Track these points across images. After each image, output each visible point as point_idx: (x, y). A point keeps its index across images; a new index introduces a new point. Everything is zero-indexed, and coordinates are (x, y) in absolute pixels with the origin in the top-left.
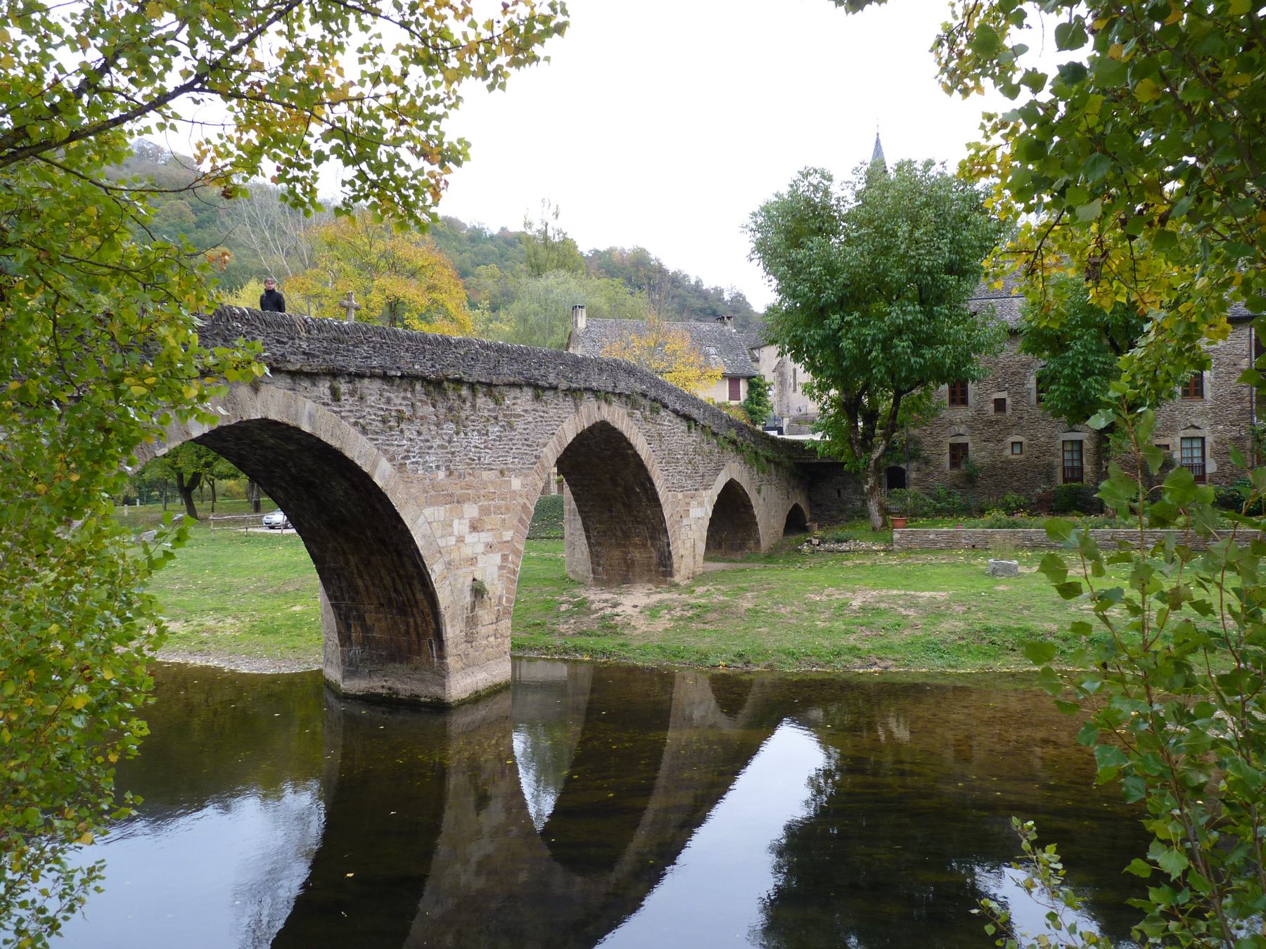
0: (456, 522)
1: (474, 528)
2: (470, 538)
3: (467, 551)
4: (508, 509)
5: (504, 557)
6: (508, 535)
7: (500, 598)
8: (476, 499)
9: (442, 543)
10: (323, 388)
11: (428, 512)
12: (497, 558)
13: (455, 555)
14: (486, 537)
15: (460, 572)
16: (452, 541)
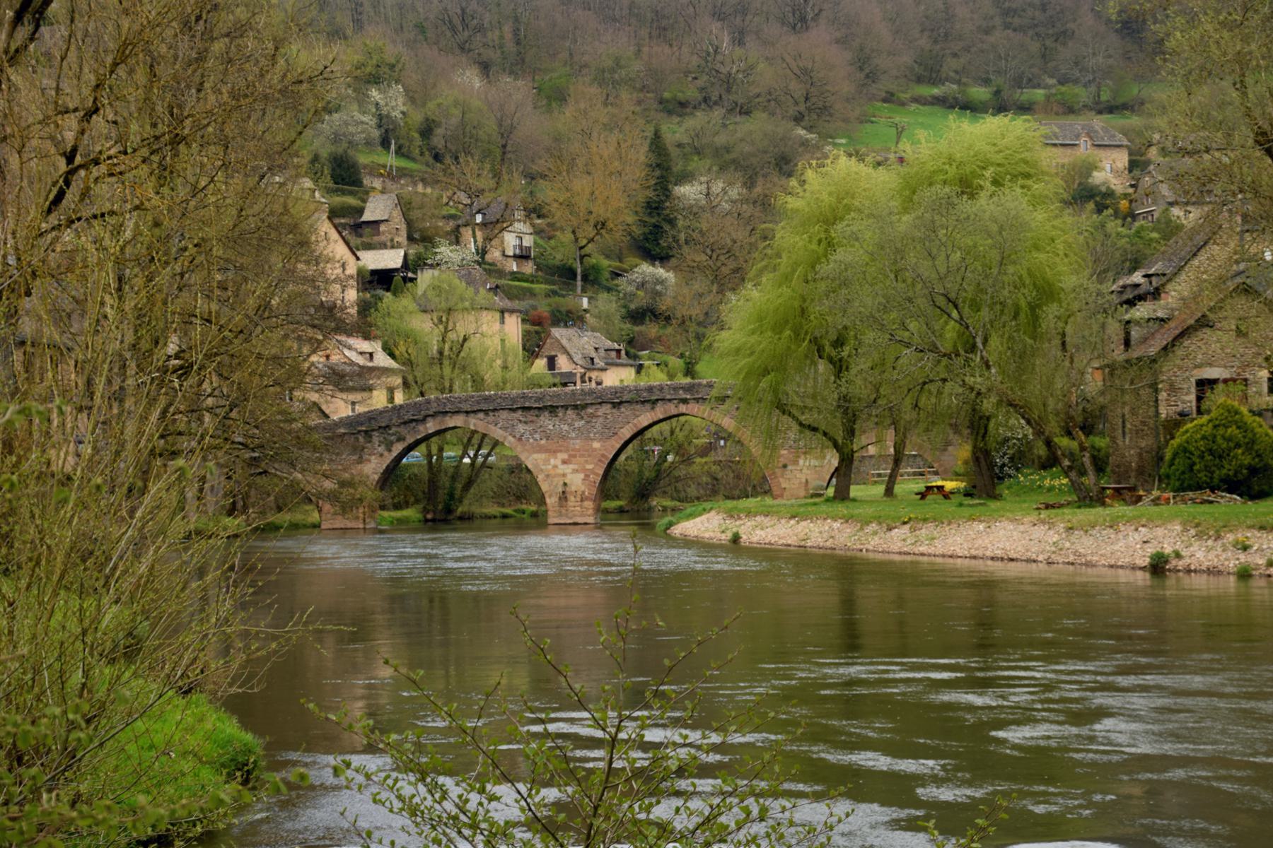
0: (552, 461)
1: (564, 462)
2: (561, 467)
3: (561, 472)
4: (589, 456)
5: (587, 476)
6: (590, 467)
7: (583, 492)
8: (567, 451)
9: (543, 467)
10: (481, 415)
11: (535, 456)
12: (582, 476)
13: (552, 472)
14: (571, 466)
15: (556, 479)
16: (550, 467)
